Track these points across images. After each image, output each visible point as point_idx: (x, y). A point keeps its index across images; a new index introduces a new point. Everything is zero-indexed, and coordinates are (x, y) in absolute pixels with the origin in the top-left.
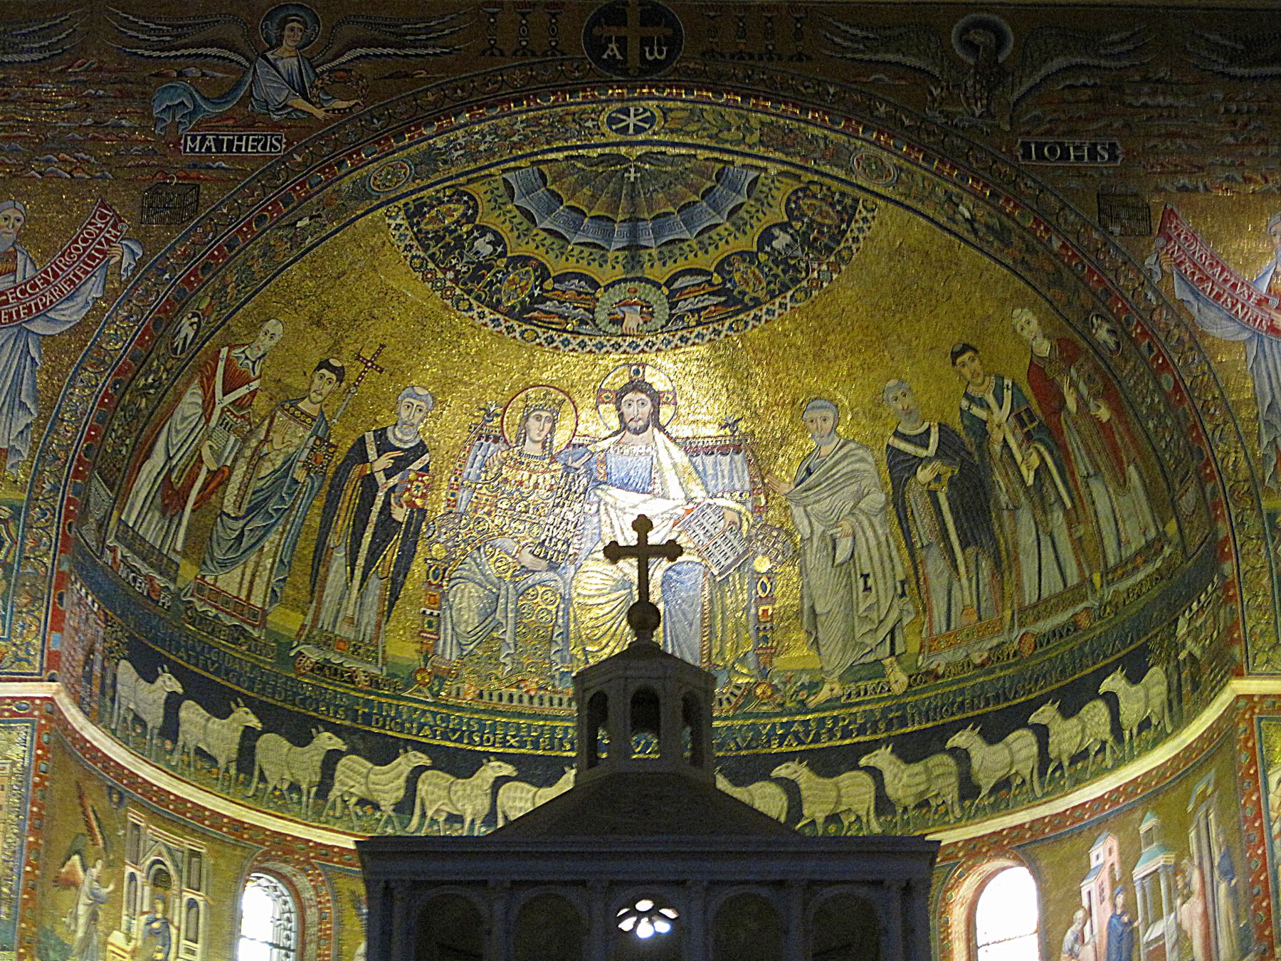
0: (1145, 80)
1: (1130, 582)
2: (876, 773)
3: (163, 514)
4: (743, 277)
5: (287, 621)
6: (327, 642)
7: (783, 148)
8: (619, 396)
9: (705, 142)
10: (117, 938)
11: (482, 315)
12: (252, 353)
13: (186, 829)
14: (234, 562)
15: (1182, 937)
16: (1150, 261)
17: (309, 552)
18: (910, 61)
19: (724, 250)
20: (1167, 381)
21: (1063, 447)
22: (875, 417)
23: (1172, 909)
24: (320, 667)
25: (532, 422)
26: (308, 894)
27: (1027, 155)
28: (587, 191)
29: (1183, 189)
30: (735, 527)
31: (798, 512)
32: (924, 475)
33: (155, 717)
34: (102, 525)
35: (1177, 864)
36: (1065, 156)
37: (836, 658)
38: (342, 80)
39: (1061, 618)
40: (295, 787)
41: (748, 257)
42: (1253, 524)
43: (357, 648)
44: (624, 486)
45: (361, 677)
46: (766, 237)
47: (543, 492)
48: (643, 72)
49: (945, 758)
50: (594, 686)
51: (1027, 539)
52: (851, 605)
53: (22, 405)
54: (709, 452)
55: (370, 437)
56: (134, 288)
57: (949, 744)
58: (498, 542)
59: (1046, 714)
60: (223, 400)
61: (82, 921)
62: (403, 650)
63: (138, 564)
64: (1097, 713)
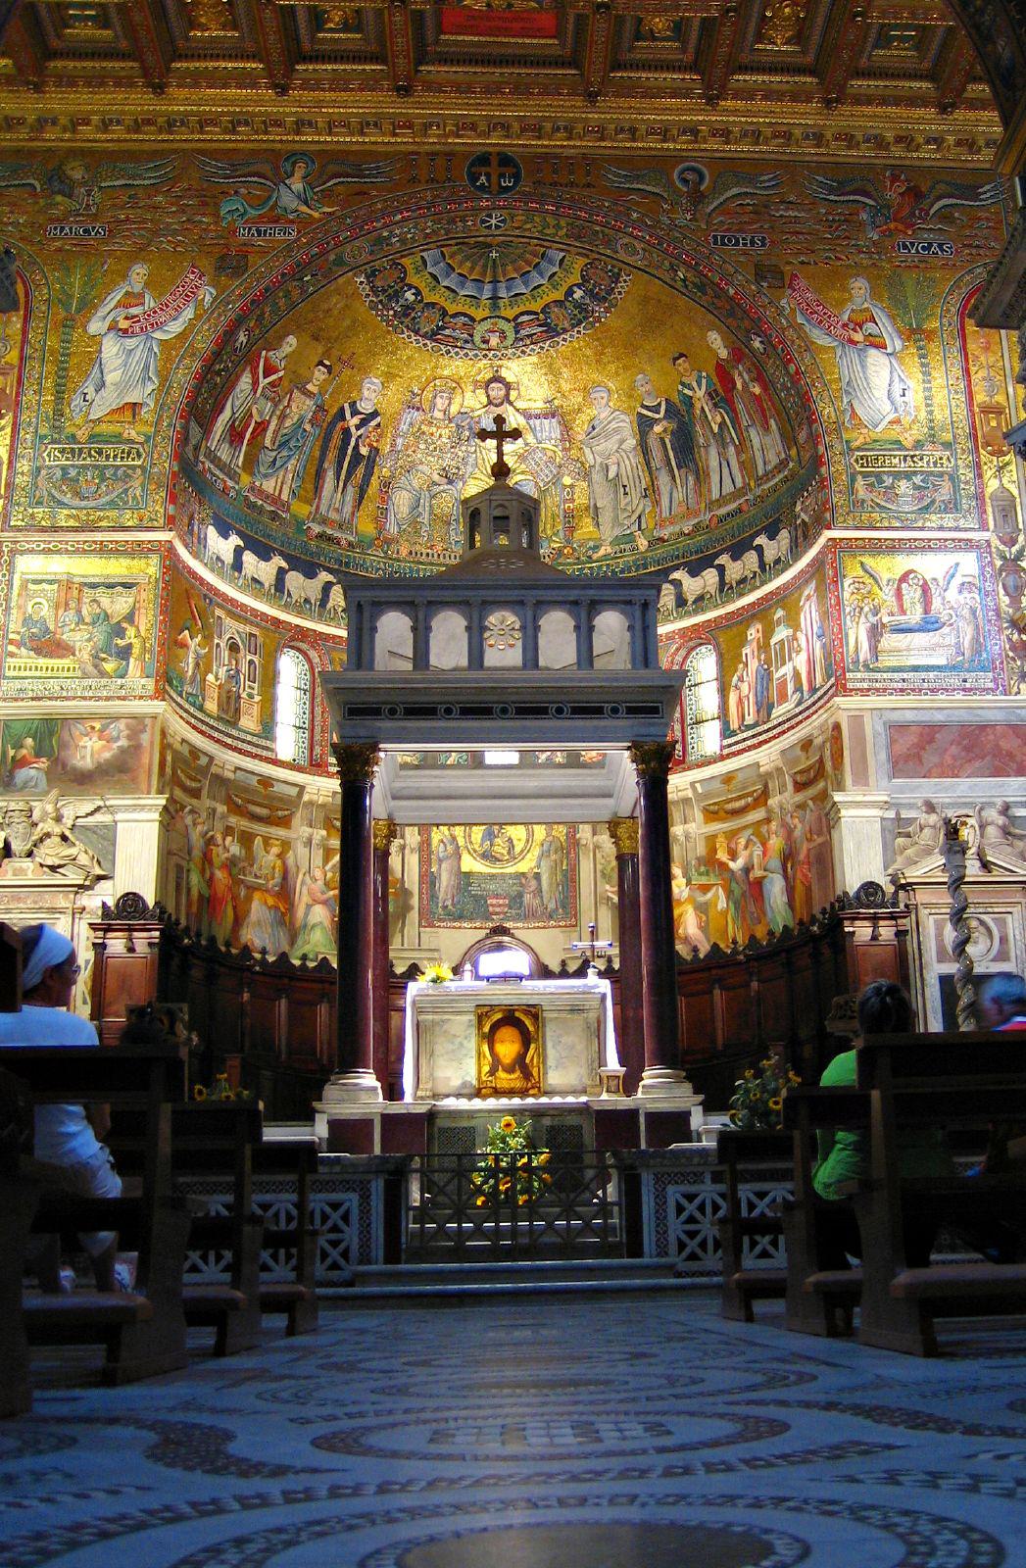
0: (782, 202)
1: (772, 483)
3: (231, 443)
5: (302, 510)
6: (324, 521)
7: (578, 238)
8: (487, 386)
9: (536, 235)
10: (210, 677)
11: (409, 337)
12: (281, 354)
13: (246, 621)
14: (271, 475)
15: (797, 675)
16: (783, 302)
17: (313, 471)
18: (649, 188)
19: (548, 299)
20: (792, 368)
21: (734, 410)
22: (630, 396)
23: (790, 659)
24: (321, 536)
25: (439, 401)
26: (316, 660)
27: (716, 243)
28: (468, 264)
29: (802, 263)
30: (552, 460)
31: (587, 451)
32: (658, 429)
33: (228, 558)
34: (197, 448)
35: (794, 634)
36: (737, 243)
37: (608, 533)
38: (327, 196)
39: (733, 506)
40: (307, 601)
41: (559, 303)
42: (838, 447)
43: (340, 527)
45: (343, 542)
46: (570, 293)
47: (444, 440)
48: (499, 193)
49: (668, 586)
50: (473, 505)
51: (714, 463)
53: (150, 379)
54: (537, 417)
55: (346, 406)
56: (212, 313)
57: (671, 577)
58: (420, 467)
59: (723, 559)
60: (263, 382)
61: (191, 666)
62: (367, 527)
63: (218, 472)
64: (751, 558)
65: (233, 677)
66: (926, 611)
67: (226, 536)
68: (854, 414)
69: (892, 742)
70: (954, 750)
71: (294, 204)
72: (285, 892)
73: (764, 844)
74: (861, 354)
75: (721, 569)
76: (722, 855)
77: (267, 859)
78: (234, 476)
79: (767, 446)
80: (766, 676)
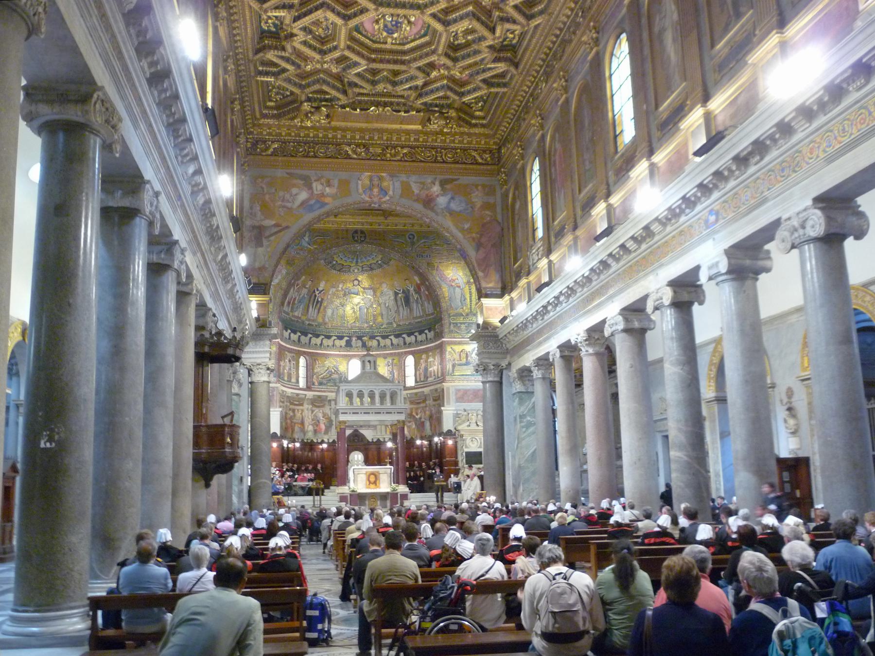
2: (391, 340)
4: (373, 266)
5: (304, 318)
24: (308, 324)
32: (400, 295)
33: (288, 337)
37: (385, 321)
38: (315, 243)
39: (419, 320)
44: (354, 294)
51: (415, 307)
52: (388, 313)
59: (416, 334)
60: (296, 288)
62: (320, 320)
64: (424, 335)
65: (290, 369)
66: (467, 360)
67: (287, 331)
68: (451, 307)
69: (456, 394)
70: (471, 396)
71: (306, 245)
72: (302, 423)
73: (425, 413)
74: (454, 289)
75: (416, 336)
76: (414, 414)
77: (298, 415)
78: (288, 314)
79: (429, 308)
80: (426, 369)
